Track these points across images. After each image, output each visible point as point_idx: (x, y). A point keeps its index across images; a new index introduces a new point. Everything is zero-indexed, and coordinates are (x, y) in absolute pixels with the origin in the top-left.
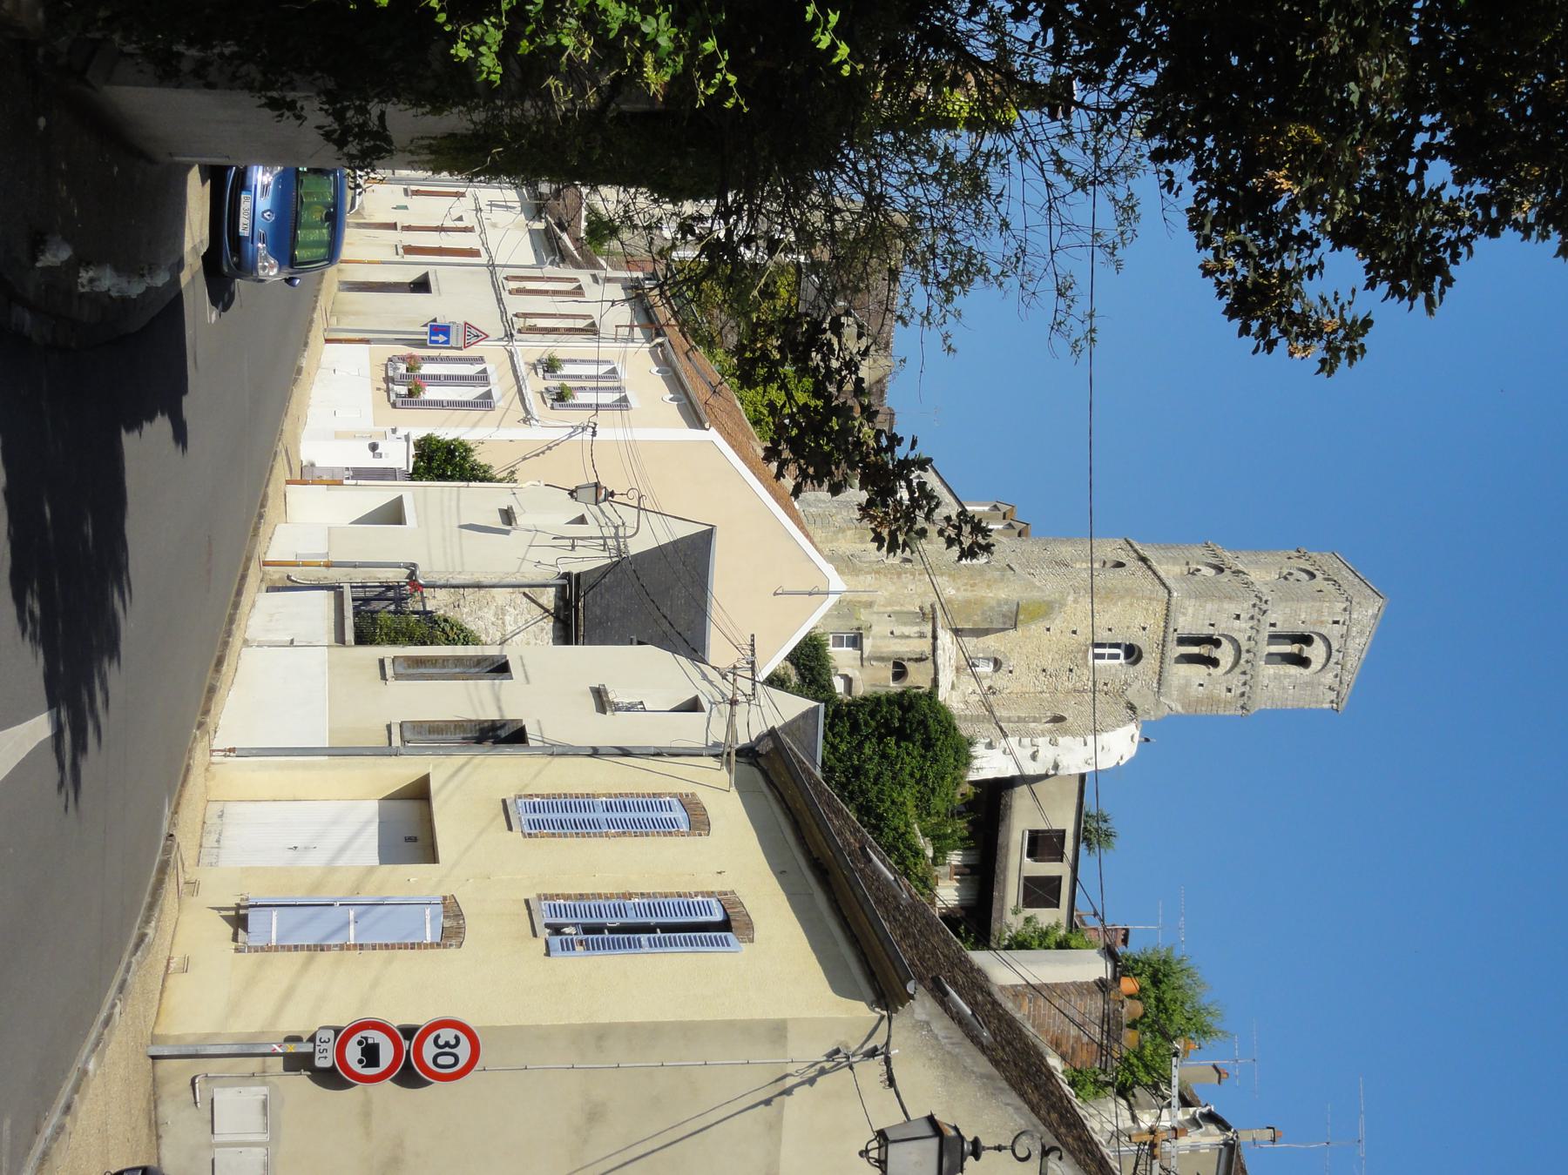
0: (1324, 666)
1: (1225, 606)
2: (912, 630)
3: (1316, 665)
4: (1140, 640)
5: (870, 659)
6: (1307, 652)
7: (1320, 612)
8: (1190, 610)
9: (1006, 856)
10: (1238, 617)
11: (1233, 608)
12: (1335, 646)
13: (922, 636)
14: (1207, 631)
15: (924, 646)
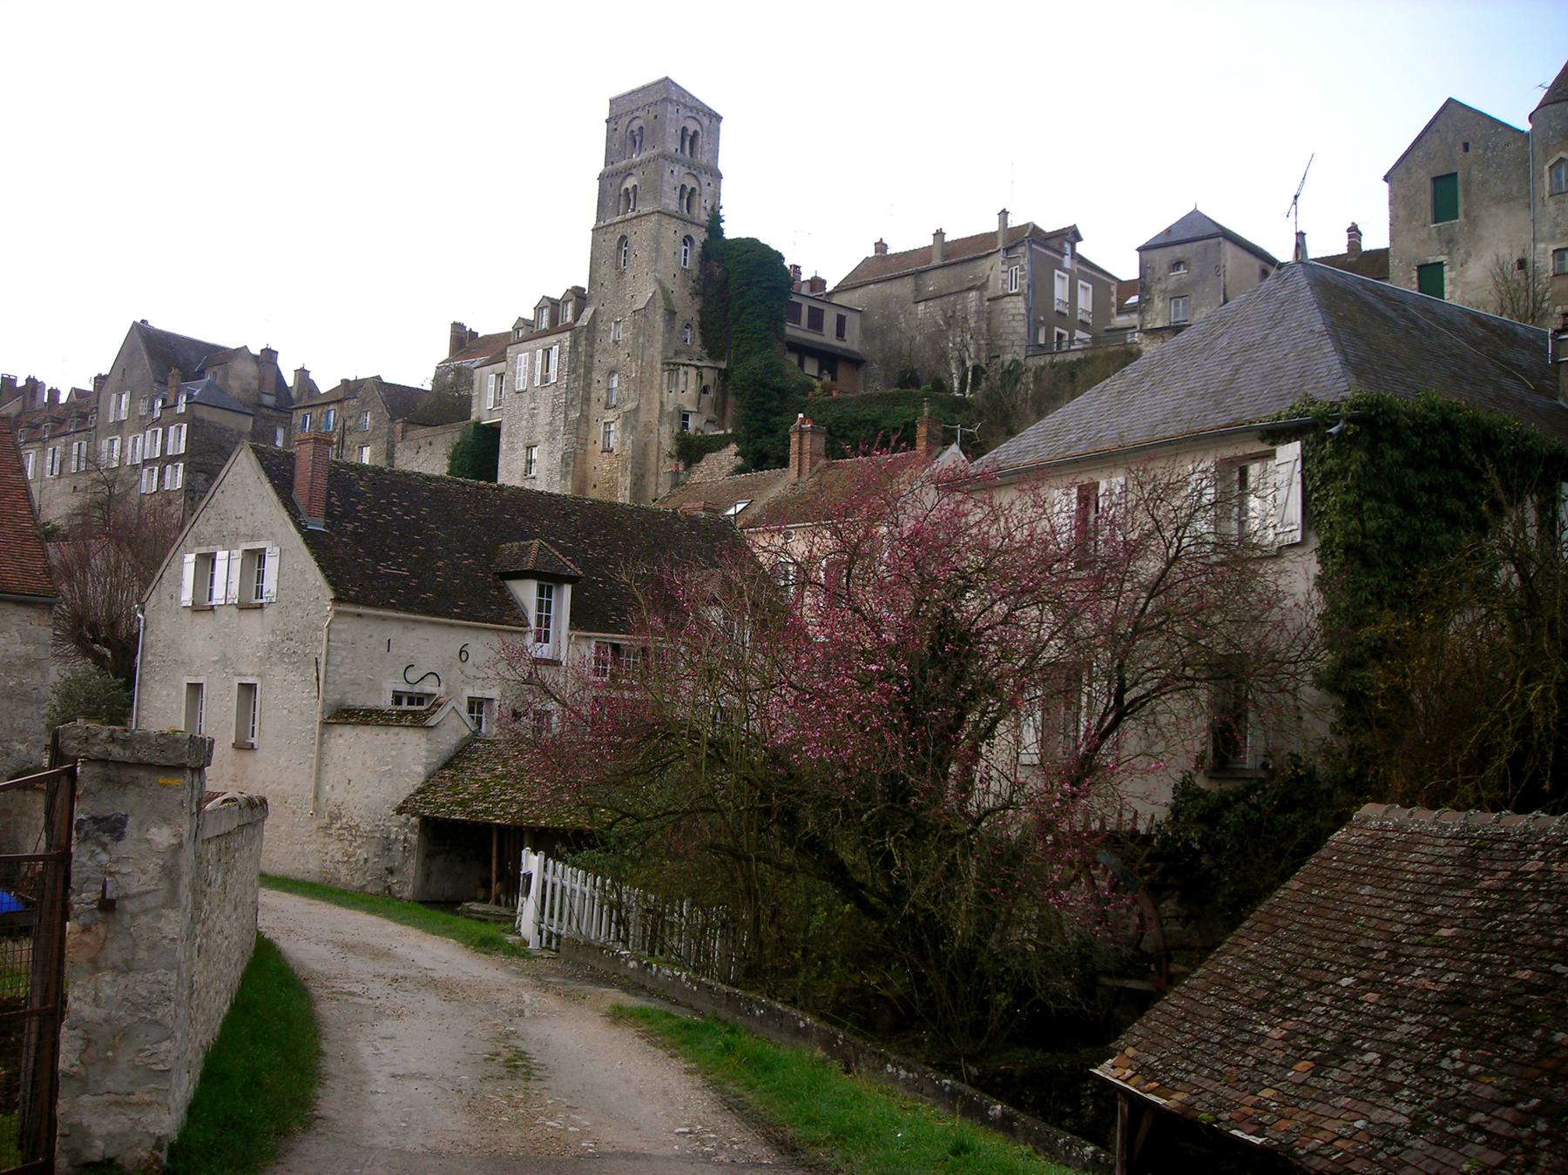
0: (700, 123)
1: (666, 178)
2: (682, 378)
3: (698, 129)
4: (681, 235)
5: (698, 408)
6: (690, 132)
7: (671, 119)
8: (667, 201)
9: (798, 338)
10: (672, 172)
11: (667, 174)
12: (690, 114)
13: (686, 373)
14: (678, 190)
15: (693, 372)
